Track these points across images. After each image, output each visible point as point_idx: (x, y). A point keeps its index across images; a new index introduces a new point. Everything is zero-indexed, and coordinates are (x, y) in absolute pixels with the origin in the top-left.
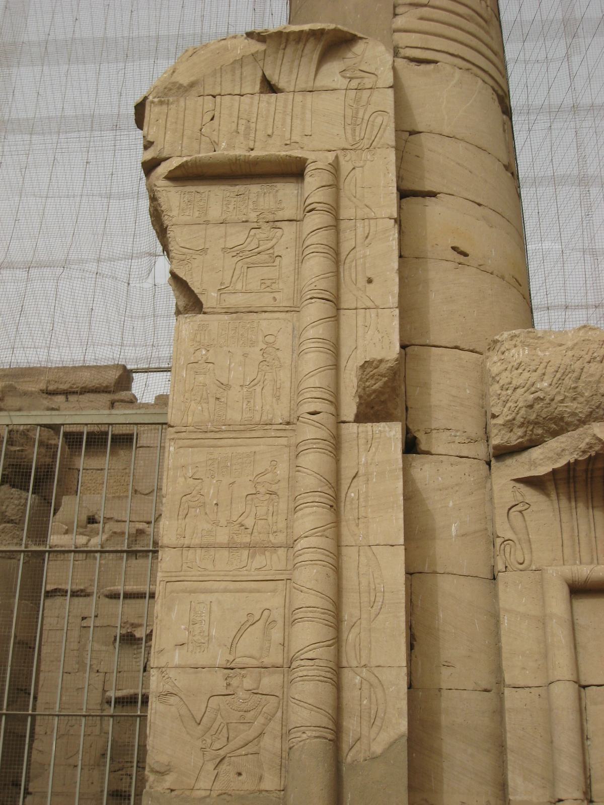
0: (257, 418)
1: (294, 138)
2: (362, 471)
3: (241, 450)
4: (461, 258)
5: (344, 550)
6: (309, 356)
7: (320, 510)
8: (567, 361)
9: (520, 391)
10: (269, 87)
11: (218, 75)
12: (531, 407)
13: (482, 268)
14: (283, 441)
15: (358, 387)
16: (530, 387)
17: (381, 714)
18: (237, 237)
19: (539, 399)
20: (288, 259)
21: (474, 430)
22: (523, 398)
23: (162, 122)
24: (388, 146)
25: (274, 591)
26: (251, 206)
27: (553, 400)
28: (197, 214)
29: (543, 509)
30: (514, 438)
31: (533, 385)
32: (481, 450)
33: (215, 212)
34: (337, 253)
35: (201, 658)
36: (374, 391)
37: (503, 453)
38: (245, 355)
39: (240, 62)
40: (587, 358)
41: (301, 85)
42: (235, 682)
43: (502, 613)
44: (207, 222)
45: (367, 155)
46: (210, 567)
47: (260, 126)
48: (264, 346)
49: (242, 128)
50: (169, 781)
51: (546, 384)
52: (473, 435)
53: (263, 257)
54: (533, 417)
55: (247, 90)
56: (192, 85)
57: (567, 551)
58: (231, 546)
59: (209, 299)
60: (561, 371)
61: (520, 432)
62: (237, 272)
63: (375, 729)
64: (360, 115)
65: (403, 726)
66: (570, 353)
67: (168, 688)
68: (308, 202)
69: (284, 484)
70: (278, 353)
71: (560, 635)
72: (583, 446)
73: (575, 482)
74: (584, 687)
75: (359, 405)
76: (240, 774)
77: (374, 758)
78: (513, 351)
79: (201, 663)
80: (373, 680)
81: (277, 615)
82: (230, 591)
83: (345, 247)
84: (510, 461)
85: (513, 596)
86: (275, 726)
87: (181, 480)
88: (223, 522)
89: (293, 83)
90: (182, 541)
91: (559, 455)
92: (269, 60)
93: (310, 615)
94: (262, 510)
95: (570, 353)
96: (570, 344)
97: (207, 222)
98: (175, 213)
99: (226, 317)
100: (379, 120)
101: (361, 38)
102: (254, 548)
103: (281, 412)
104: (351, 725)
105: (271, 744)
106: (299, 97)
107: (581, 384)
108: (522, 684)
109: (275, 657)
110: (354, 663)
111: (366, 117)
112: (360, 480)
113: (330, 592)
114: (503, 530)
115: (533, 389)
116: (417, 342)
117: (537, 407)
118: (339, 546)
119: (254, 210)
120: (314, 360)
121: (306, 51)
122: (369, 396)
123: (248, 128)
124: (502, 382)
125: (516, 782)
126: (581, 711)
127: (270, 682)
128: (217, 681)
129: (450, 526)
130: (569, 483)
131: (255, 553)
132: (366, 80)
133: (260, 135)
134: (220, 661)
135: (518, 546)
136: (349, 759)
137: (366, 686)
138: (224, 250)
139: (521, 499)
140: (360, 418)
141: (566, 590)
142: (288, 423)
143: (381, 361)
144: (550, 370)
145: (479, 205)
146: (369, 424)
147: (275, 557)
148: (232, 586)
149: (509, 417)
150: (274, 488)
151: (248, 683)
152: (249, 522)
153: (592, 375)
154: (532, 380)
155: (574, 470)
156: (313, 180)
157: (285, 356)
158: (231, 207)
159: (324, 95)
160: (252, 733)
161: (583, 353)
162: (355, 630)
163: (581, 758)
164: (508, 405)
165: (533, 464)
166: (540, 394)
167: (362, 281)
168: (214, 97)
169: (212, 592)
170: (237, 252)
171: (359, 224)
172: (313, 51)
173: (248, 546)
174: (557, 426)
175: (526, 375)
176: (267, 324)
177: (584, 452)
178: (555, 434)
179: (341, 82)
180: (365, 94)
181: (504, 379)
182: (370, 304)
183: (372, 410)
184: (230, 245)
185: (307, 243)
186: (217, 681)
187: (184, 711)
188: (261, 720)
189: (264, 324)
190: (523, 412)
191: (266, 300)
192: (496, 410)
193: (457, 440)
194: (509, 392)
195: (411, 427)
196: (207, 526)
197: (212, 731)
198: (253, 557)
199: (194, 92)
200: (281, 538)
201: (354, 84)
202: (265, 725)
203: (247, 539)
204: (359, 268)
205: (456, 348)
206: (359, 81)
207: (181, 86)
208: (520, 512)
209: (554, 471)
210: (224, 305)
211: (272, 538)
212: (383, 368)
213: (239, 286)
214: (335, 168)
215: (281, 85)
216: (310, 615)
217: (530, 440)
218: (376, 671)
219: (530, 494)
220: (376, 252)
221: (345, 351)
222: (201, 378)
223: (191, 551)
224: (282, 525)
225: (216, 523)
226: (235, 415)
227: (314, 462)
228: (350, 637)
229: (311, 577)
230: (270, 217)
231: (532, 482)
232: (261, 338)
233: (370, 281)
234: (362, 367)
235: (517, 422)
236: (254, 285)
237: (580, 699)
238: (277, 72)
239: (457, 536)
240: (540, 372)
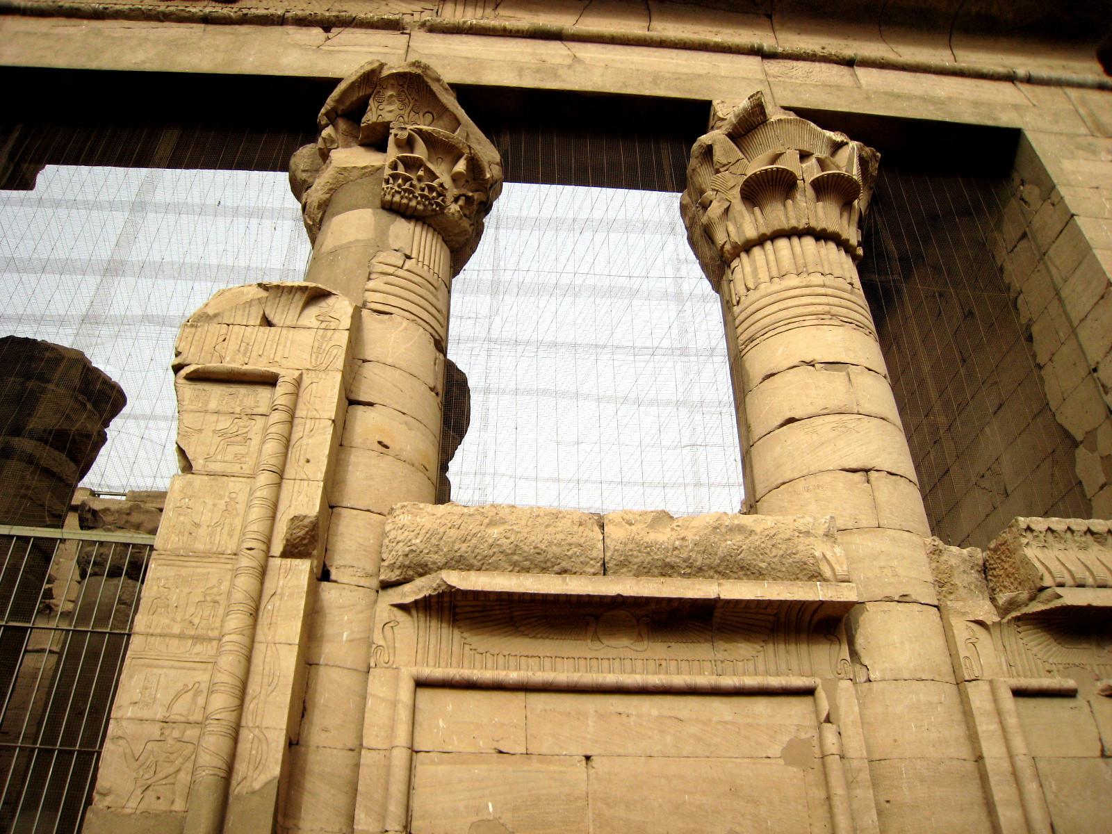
0: (215, 549)
1: (276, 359)
2: (279, 591)
3: (199, 570)
4: (384, 450)
5: (257, 645)
6: (254, 509)
7: (242, 616)
8: (435, 526)
9: (401, 544)
10: (267, 322)
11: (234, 311)
12: (407, 555)
13: (398, 457)
14: (229, 566)
15: (287, 533)
16: (408, 542)
17: (263, 762)
18: (225, 423)
19: (412, 551)
20: (255, 442)
21: (370, 568)
22: (402, 549)
23: (190, 339)
24: (338, 370)
25: (205, 670)
26: (238, 402)
27: (421, 552)
28: (200, 405)
29: (407, 626)
30: (393, 576)
31: (410, 540)
32: (374, 583)
33: (213, 405)
34: (288, 440)
35: (146, 714)
36: (299, 537)
37: (386, 586)
38: (214, 505)
39: (250, 303)
40: (449, 525)
41: (288, 323)
42: (167, 732)
43: (368, 697)
44: (206, 411)
45: (322, 375)
46: (164, 650)
47: (255, 348)
48: (228, 500)
49: (242, 349)
50: (108, 801)
51: (418, 541)
52: (370, 572)
53: (239, 439)
54: (407, 563)
56: (216, 315)
57: (420, 656)
58: (181, 637)
59: (198, 465)
60: (430, 533)
61: (398, 572)
62: (220, 447)
63: (257, 772)
64: (323, 347)
65: (276, 771)
66: (438, 521)
67: (120, 733)
68: (275, 403)
69: (225, 596)
70: (237, 505)
71: (403, 715)
72: (435, 585)
73: (430, 610)
74: (417, 752)
75: (285, 547)
76: (159, 798)
77: (254, 792)
78: (401, 517)
79: (146, 717)
80: (261, 736)
81: (204, 687)
82: (175, 668)
83: (295, 436)
84: (391, 592)
85: (378, 685)
86: (189, 765)
87: (155, 588)
88: (178, 619)
89: (282, 321)
90: (148, 630)
91: (420, 591)
92: (269, 303)
93: (222, 688)
94: (206, 613)
95: (438, 521)
96: (439, 515)
97: (206, 411)
99: (206, 478)
100: (335, 352)
101: (334, 294)
102: (197, 639)
103: (231, 546)
104: (241, 768)
105: (184, 778)
106: (285, 331)
107: (442, 543)
108: (374, 747)
109: (197, 716)
110: (251, 724)
111: (327, 349)
112: (277, 597)
113: (240, 673)
114: (378, 639)
115: (409, 544)
116: (340, 505)
117: (410, 556)
118: (253, 641)
119: (239, 406)
120: (258, 512)
121: (295, 300)
122: (295, 540)
123: (247, 349)
124: (390, 537)
125: (360, 815)
126: (411, 769)
127: (191, 733)
128: (155, 731)
129: (342, 634)
130: (426, 610)
131: (196, 642)
132: (332, 324)
133: (254, 354)
134: (159, 716)
135: (387, 651)
136: (236, 792)
137: (256, 741)
138: (214, 431)
139: (393, 618)
140: (285, 555)
141: (412, 684)
142: (235, 554)
143: (305, 517)
144: (423, 531)
145: (404, 414)
146: (289, 560)
147: (209, 646)
148: (177, 664)
149: (392, 562)
150: (218, 598)
151: (176, 734)
152: (196, 621)
153: (450, 537)
154: (410, 537)
155: (430, 602)
156: (281, 389)
157: (241, 508)
158: (224, 402)
159: (302, 331)
160: (172, 770)
161: (447, 522)
162: (255, 701)
163: (405, 802)
164: (394, 553)
165: (404, 595)
166: (414, 548)
167: (302, 461)
168: (228, 325)
169: (162, 667)
170: (222, 433)
171: (308, 422)
172: (299, 300)
173: (192, 637)
174: (423, 570)
175: (406, 533)
176: (234, 485)
177: (435, 589)
178: (421, 575)
179: (315, 323)
181: (392, 535)
182: (305, 477)
183: (293, 550)
184: (218, 428)
185: (269, 432)
186: (155, 731)
187: (128, 750)
188: (180, 760)
189: (231, 484)
190: (401, 559)
191: (235, 469)
192: (384, 556)
193: (358, 574)
194: (394, 544)
195: (327, 563)
196: (167, 621)
197: (145, 767)
198: (194, 644)
200: (216, 634)
201: (323, 325)
202: (183, 764)
203: (193, 633)
204: (302, 452)
205: (368, 511)
206: (327, 323)
207: (208, 315)
208: (392, 627)
209: (416, 602)
210: (208, 469)
211: (209, 632)
212: (306, 521)
213: (219, 457)
214: (298, 382)
215: (275, 321)
216: (222, 688)
217: (405, 579)
218: (264, 731)
219: (399, 614)
220: (316, 443)
221: (281, 508)
222: (182, 518)
223: (154, 638)
224: (218, 624)
225: (174, 620)
226: (200, 546)
227: (245, 583)
228: (250, 706)
229: (229, 662)
230: (249, 412)
231: (402, 607)
232: (227, 494)
233: (308, 461)
234: (292, 519)
235: (397, 566)
236: (229, 457)
237: (411, 760)
238: (273, 312)
239: (347, 641)
240: (416, 532)
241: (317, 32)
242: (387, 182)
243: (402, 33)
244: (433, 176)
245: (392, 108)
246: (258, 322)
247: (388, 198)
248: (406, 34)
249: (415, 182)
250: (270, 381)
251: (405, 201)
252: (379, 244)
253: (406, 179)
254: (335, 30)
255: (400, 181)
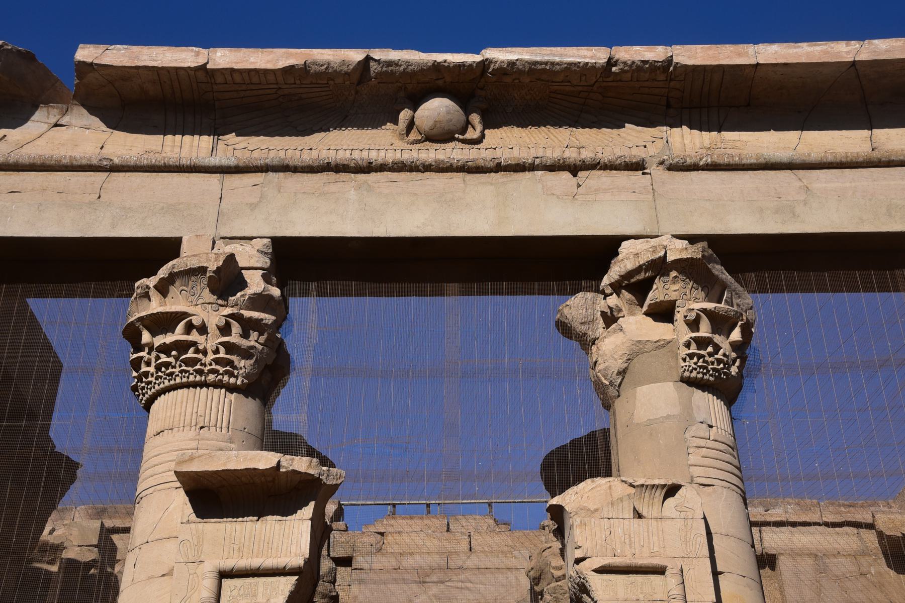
1: (656, 549)
41: (655, 515)
49: (627, 541)
55: (627, 516)
56: (596, 510)
98: (600, 593)
106: (654, 523)
119: (641, 593)
123: (630, 540)
133: (637, 545)
179: (675, 514)
180: (690, 522)
199: (597, 515)
201: (683, 515)
207: (589, 510)
215: (644, 513)
230: (651, 598)
241: (566, 175)
242: (684, 360)
243: (644, 174)
244: (717, 348)
245: (676, 287)
246: (632, 516)
247: (687, 374)
248: (647, 174)
249: (707, 358)
250: (660, 571)
251: (700, 376)
252: (687, 418)
253: (700, 357)
254: (581, 174)
255: (695, 359)
